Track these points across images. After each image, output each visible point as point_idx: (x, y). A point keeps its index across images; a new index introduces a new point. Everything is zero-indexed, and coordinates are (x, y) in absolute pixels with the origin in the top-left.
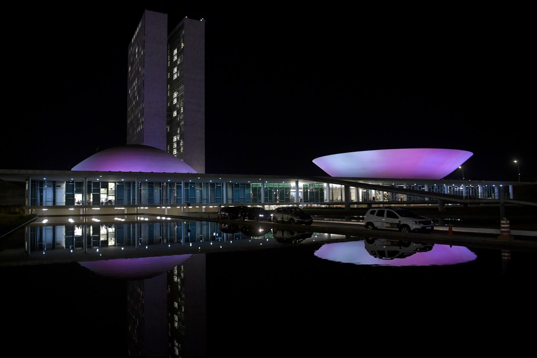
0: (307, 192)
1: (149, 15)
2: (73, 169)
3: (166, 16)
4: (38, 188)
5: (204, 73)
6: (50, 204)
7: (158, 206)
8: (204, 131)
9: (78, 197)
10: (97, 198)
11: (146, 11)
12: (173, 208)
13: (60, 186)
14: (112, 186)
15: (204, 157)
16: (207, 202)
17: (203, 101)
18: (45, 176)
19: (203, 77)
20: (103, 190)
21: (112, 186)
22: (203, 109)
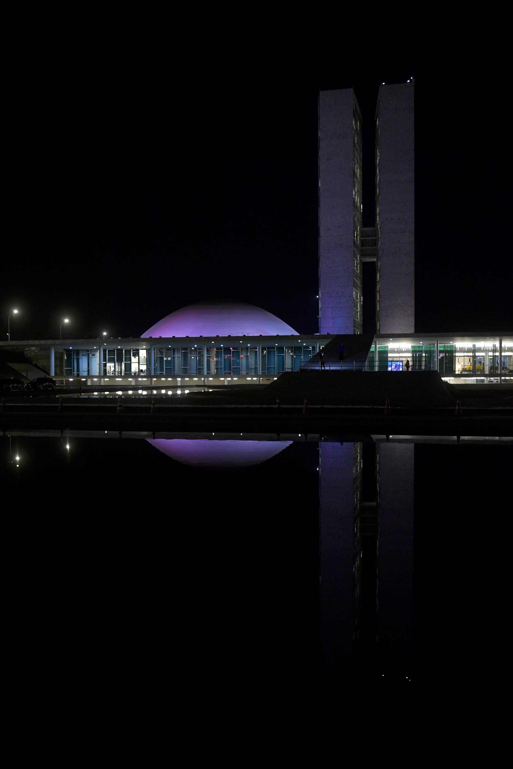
0: (421, 356)
1: (327, 99)
2: (142, 336)
3: (350, 91)
4: (75, 357)
5: (413, 168)
6: (86, 374)
7: (179, 376)
8: (413, 260)
9: (110, 366)
10: (128, 367)
11: (321, 92)
12: (125, 379)
13: (94, 355)
14: (143, 353)
15: (413, 303)
16: (256, 372)
17: (412, 214)
18: (71, 345)
19: (412, 175)
20: (134, 360)
21: (143, 353)
22: (412, 227)
